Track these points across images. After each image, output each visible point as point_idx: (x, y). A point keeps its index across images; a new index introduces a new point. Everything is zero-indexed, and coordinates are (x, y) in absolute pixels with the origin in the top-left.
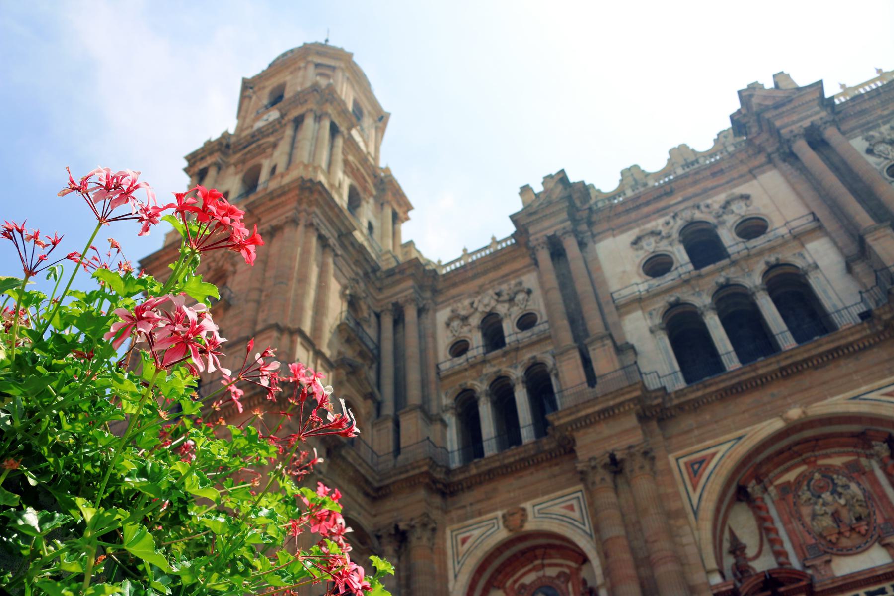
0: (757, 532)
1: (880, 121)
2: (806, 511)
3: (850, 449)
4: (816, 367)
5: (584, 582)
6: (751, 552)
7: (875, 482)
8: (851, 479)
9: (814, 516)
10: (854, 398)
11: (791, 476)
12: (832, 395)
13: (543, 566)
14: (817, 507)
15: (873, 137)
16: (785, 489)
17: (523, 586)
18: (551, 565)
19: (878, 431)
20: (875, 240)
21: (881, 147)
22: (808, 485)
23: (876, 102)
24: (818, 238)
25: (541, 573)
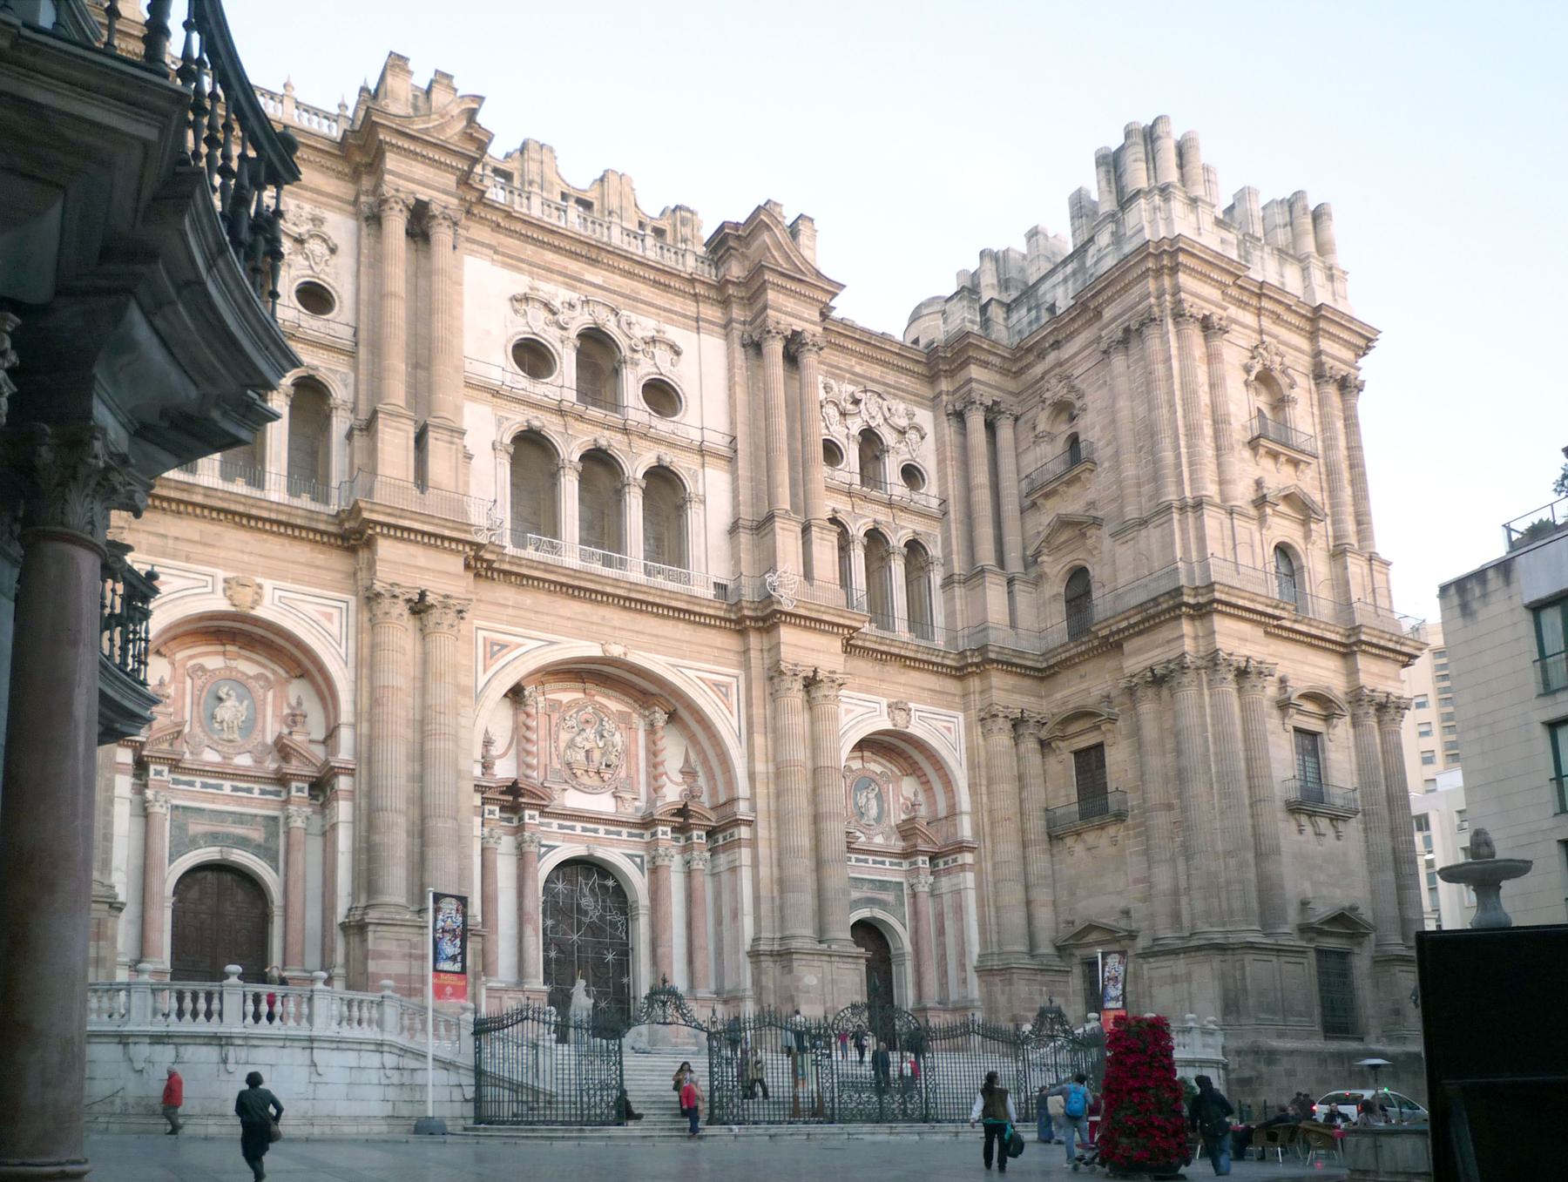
0: (509, 734)
1: (848, 375)
2: (565, 736)
3: (630, 701)
4: (657, 615)
5: (299, 703)
6: (495, 751)
7: (636, 741)
8: (617, 728)
9: (571, 745)
10: (673, 666)
11: (566, 697)
12: (657, 652)
13: (240, 656)
14: (578, 739)
15: (832, 389)
16: (555, 705)
17: (202, 668)
18: (248, 659)
19: (668, 701)
20: (783, 529)
21: (831, 411)
22: (577, 713)
23: (860, 348)
24: (722, 469)
25: (233, 663)
